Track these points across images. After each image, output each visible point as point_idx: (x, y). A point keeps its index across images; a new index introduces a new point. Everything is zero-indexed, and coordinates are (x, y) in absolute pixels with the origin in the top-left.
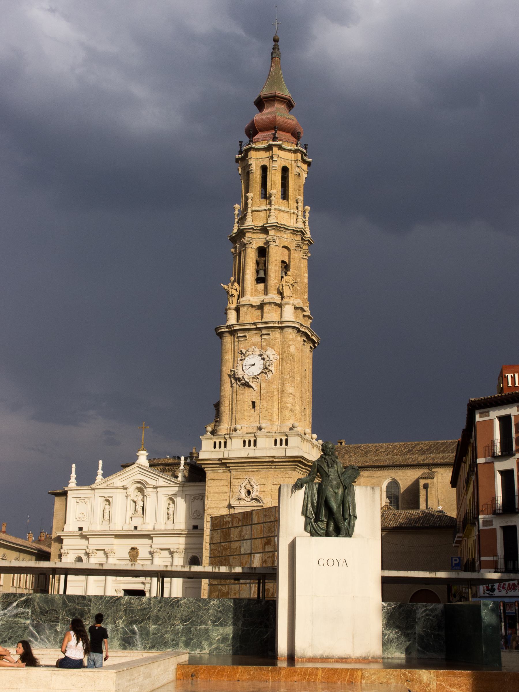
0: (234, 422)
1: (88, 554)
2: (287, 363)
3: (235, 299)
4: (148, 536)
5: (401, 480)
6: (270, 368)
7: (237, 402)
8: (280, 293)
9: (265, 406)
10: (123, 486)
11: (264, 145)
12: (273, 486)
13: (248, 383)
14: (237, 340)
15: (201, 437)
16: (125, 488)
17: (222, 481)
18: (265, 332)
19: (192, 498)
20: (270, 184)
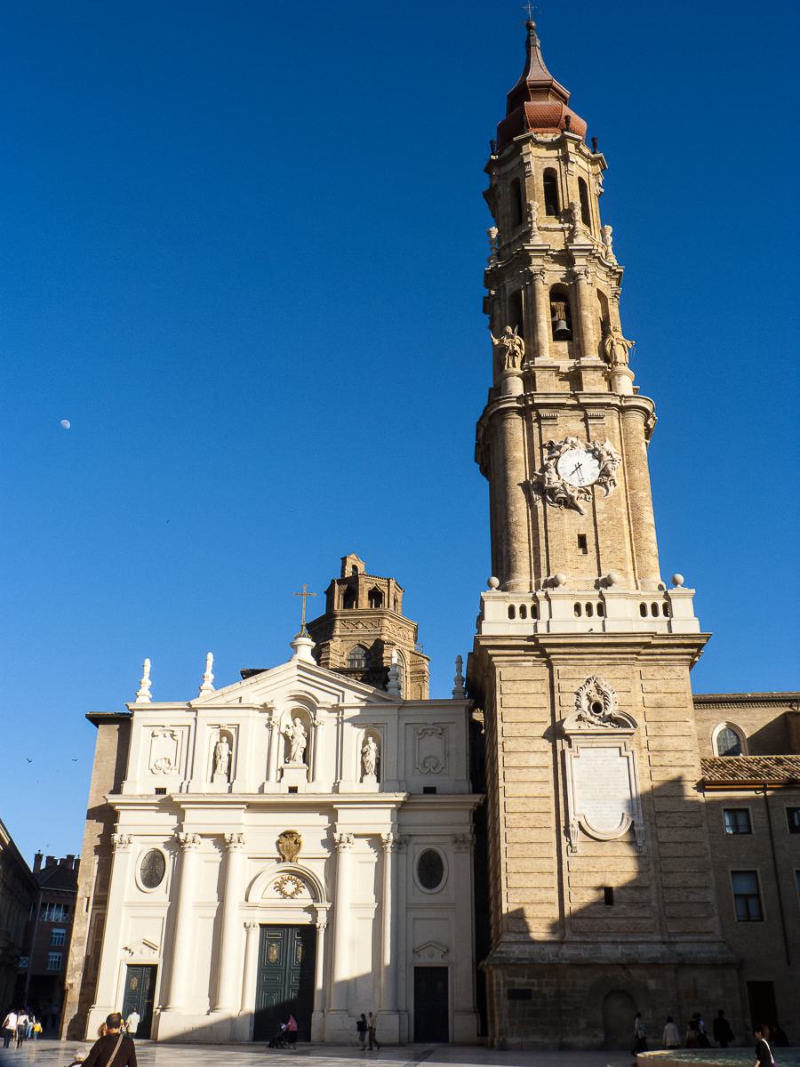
0: (544, 572)
1: (182, 844)
2: (640, 471)
3: (518, 361)
4: (328, 809)
5: (745, 725)
6: (613, 473)
7: (549, 534)
8: (607, 357)
9: (609, 543)
10: (265, 705)
11: (549, 137)
12: (645, 695)
13: (572, 498)
14: (535, 425)
15: (482, 594)
16: (266, 709)
17: (533, 684)
18: (591, 412)
19: (420, 731)
20: (565, 194)
